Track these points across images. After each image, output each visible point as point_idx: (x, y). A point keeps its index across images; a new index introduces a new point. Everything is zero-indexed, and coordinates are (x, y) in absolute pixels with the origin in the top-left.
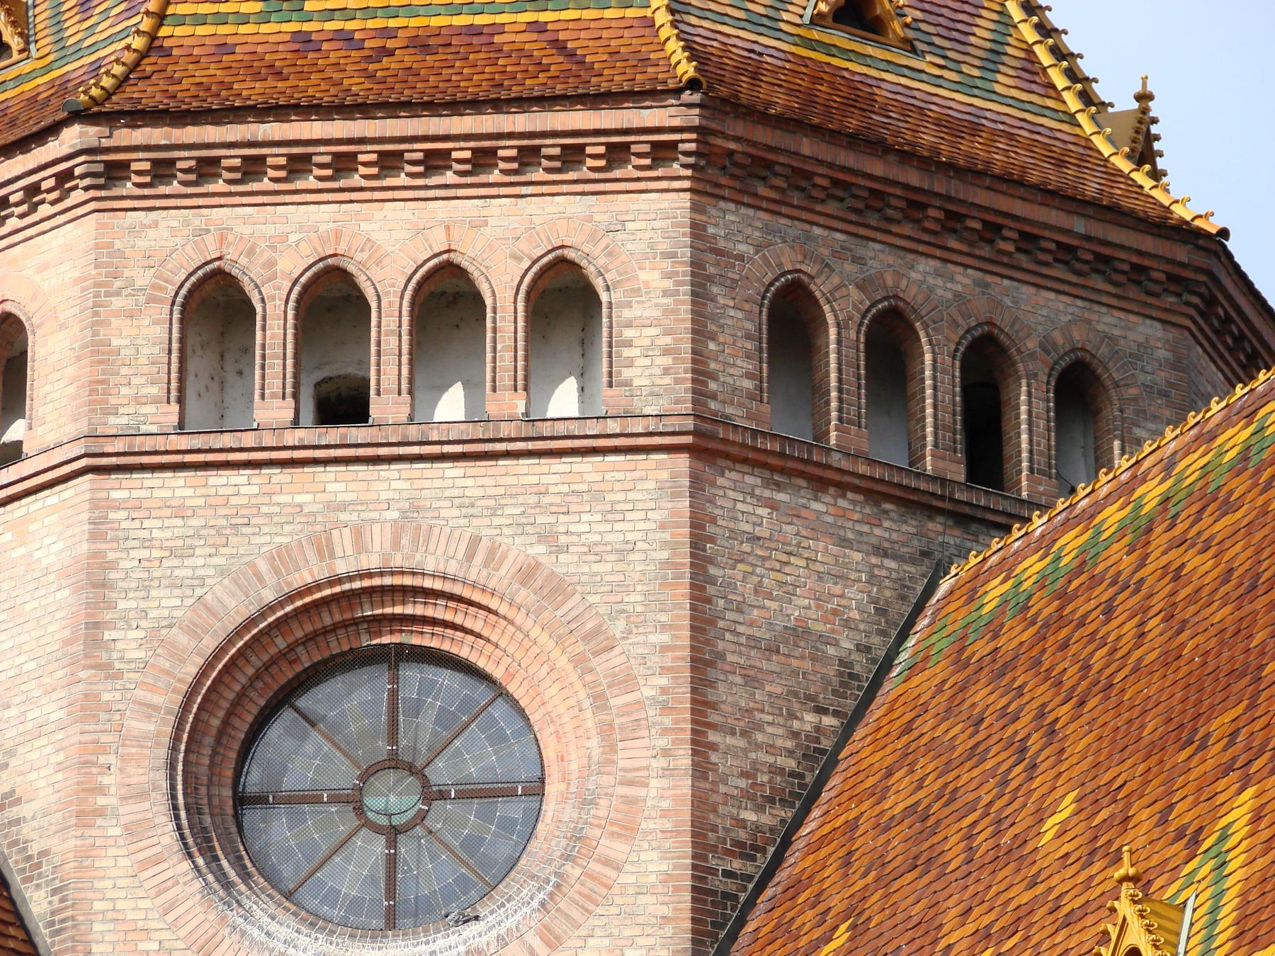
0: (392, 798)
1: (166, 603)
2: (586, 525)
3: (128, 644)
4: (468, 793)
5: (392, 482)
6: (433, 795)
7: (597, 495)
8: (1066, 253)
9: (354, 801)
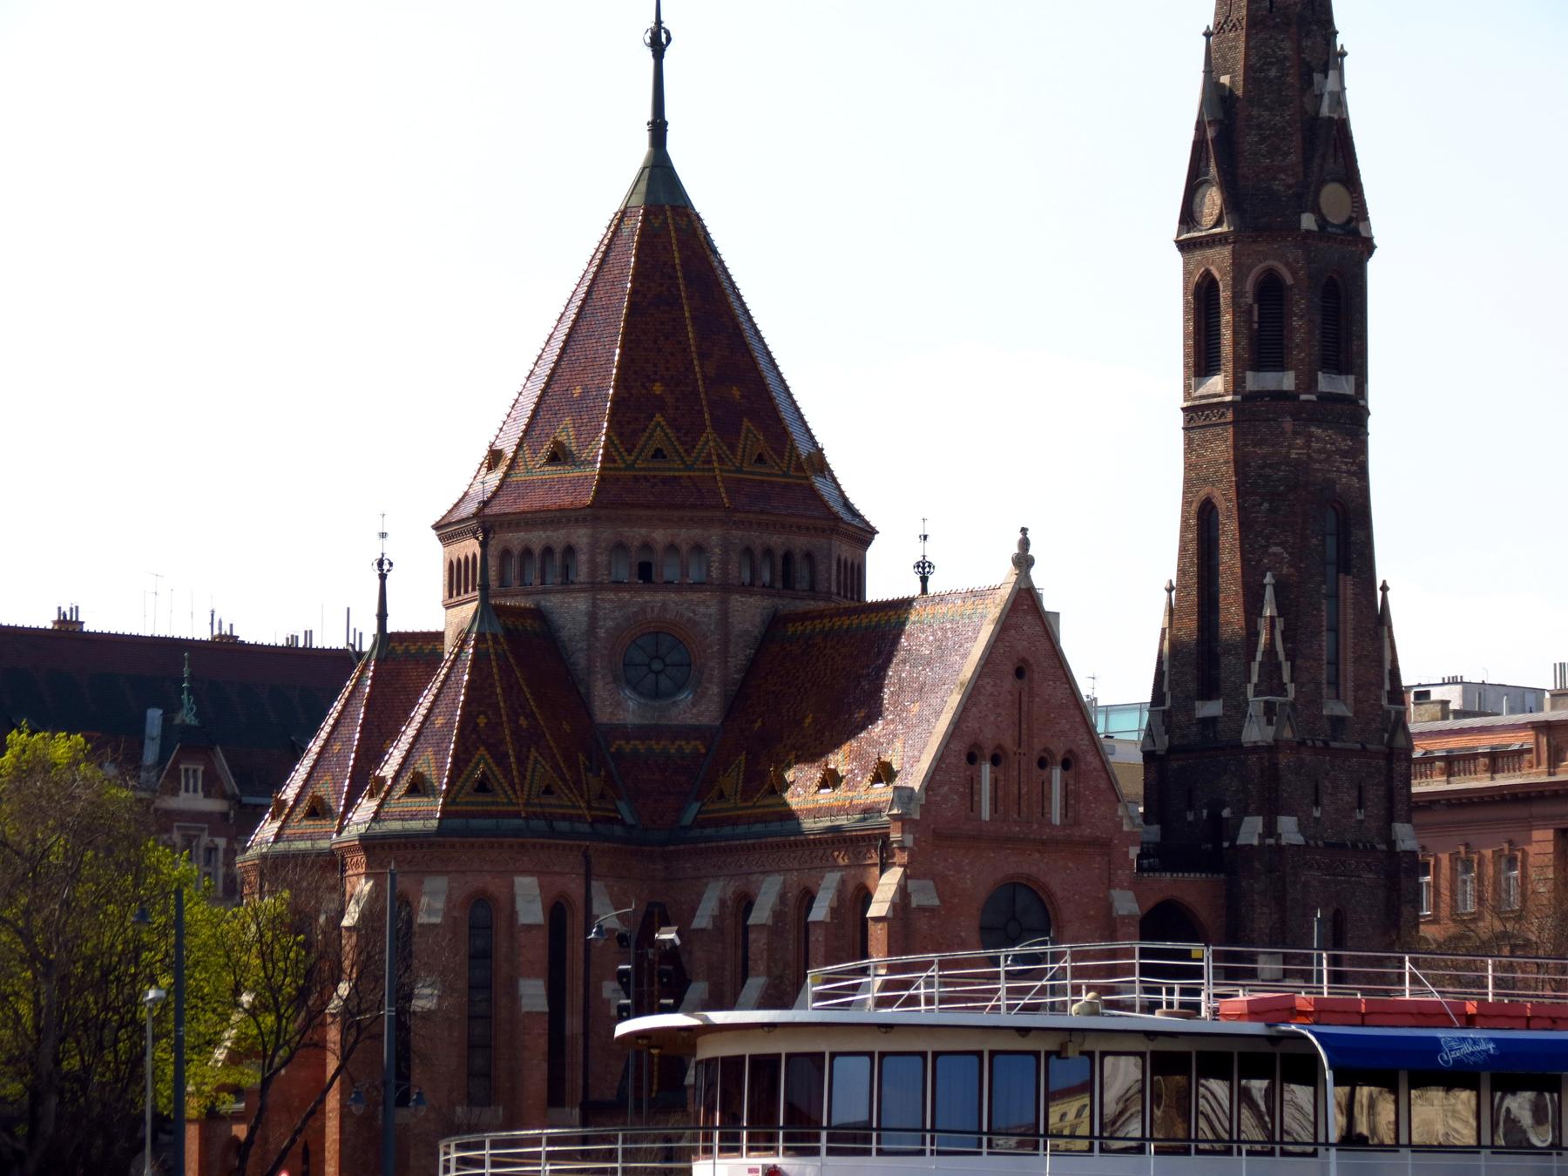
0: (657, 666)
1: (610, 623)
2: (702, 609)
3: (602, 633)
4: (674, 665)
5: (659, 597)
6: (666, 665)
7: (704, 602)
8: (808, 529)
9: (649, 665)
